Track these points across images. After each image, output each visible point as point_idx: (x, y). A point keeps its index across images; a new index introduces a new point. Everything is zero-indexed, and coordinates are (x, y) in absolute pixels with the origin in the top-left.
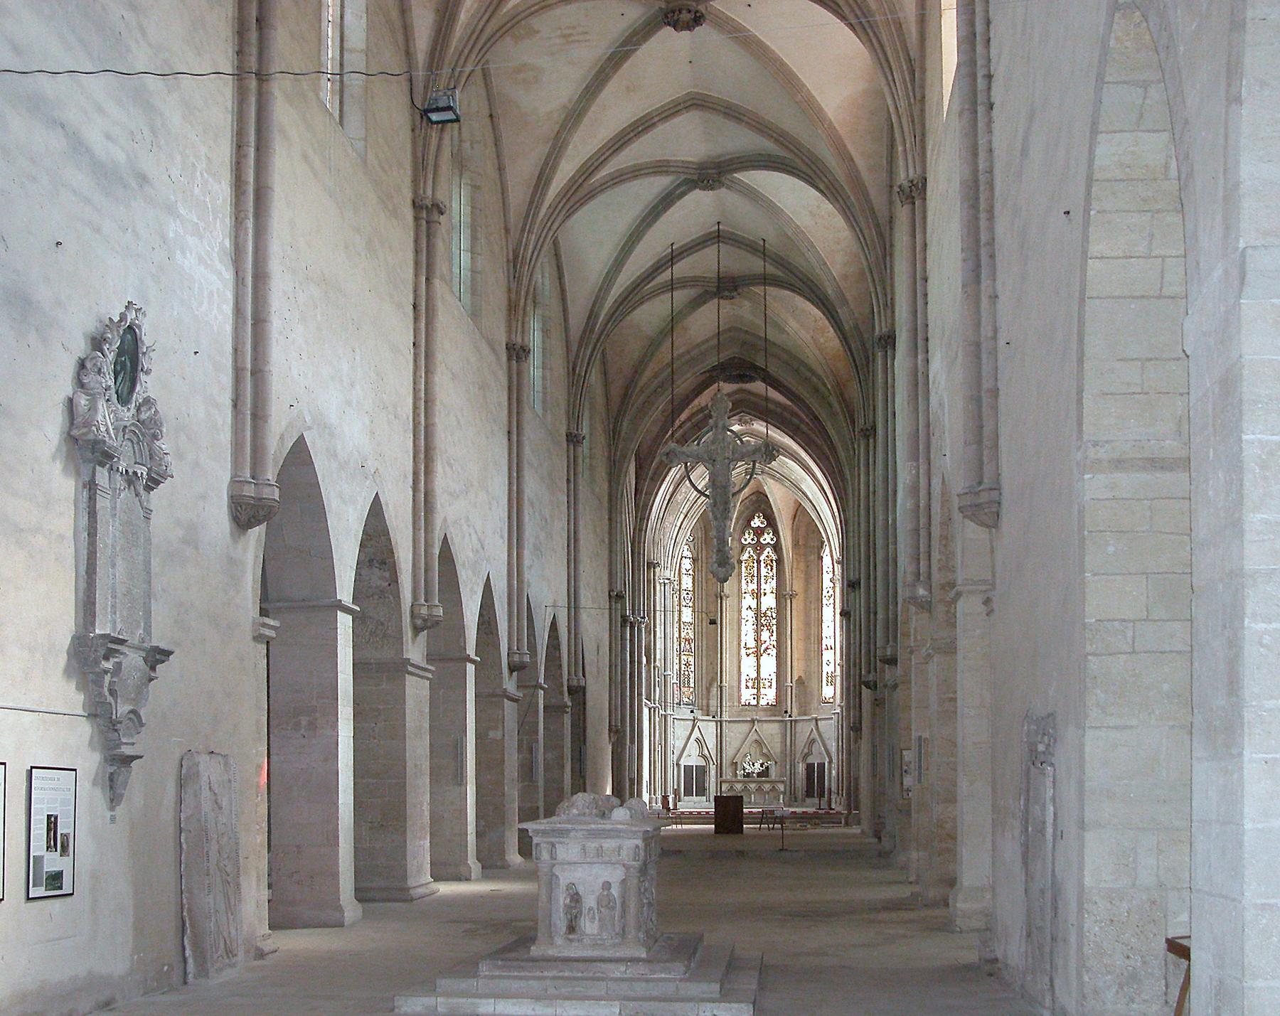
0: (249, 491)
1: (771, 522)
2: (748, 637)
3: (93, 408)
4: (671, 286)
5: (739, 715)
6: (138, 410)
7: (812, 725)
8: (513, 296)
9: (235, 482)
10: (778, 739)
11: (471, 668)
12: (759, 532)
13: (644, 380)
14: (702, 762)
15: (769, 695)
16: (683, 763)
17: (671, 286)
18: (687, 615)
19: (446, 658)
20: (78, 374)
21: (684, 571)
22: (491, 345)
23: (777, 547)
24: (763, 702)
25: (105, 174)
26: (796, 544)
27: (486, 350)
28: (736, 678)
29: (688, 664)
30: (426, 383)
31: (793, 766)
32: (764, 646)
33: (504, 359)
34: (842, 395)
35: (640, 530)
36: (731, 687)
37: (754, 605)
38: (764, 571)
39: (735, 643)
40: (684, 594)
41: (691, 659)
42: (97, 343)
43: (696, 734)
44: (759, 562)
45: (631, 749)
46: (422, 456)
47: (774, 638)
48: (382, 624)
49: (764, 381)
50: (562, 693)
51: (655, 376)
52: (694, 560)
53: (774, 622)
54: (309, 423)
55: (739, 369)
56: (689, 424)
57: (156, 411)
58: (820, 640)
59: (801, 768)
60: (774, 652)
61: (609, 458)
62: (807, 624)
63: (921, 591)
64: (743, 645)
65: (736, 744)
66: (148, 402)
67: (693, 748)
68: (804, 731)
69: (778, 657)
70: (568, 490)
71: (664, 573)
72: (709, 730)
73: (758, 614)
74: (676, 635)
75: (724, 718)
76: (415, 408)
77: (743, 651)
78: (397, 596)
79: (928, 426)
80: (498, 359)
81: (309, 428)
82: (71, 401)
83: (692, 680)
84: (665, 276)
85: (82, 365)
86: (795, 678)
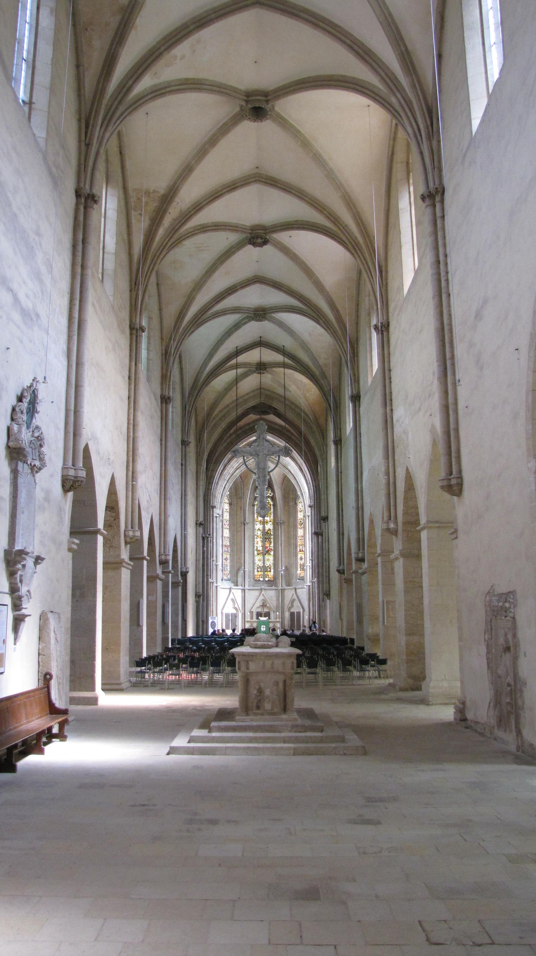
0: (72, 473)
1: (270, 486)
3: (20, 431)
4: (237, 366)
5: (253, 586)
6: (33, 431)
7: (293, 592)
8: (164, 371)
9: (64, 468)
10: (275, 599)
11: (145, 562)
13: (216, 412)
14: (234, 611)
16: (225, 612)
17: (237, 366)
18: (227, 533)
19: (136, 558)
20: (12, 414)
21: (225, 510)
22: (155, 395)
23: (273, 498)
24: (267, 579)
25: (25, 313)
27: (153, 398)
28: (252, 566)
29: (226, 559)
30: (134, 416)
31: (283, 613)
33: (160, 403)
34: (318, 423)
35: (208, 489)
36: (250, 571)
37: (261, 528)
39: (252, 548)
40: (225, 522)
41: (228, 557)
42: (20, 399)
43: (231, 596)
45: (203, 604)
46: (131, 453)
47: (272, 545)
48: (110, 540)
49: (274, 414)
50: (178, 575)
51: (221, 411)
52: (230, 504)
53: (272, 537)
54: (90, 437)
55: (263, 409)
56: (234, 435)
57: (42, 433)
58: (296, 547)
59: (287, 615)
60: (272, 553)
61: (197, 452)
63: (392, 526)
64: (256, 548)
65: (253, 601)
66: (37, 427)
67: (230, 603)
68: (289, 594)
69: (275, 556)
70: (182, 469)
71: (217, 511)
72: (237, 593)
74: (221, 544)
75: (247, 587)
76: (128, 428)
77: (256, 553)
78: (118, 526)
79: (393, 442)
80: (157, 403)
81: (90, 440)
82: (9, 429)
83: (228, 568)
84: (233, 362)
85: (14, 409)
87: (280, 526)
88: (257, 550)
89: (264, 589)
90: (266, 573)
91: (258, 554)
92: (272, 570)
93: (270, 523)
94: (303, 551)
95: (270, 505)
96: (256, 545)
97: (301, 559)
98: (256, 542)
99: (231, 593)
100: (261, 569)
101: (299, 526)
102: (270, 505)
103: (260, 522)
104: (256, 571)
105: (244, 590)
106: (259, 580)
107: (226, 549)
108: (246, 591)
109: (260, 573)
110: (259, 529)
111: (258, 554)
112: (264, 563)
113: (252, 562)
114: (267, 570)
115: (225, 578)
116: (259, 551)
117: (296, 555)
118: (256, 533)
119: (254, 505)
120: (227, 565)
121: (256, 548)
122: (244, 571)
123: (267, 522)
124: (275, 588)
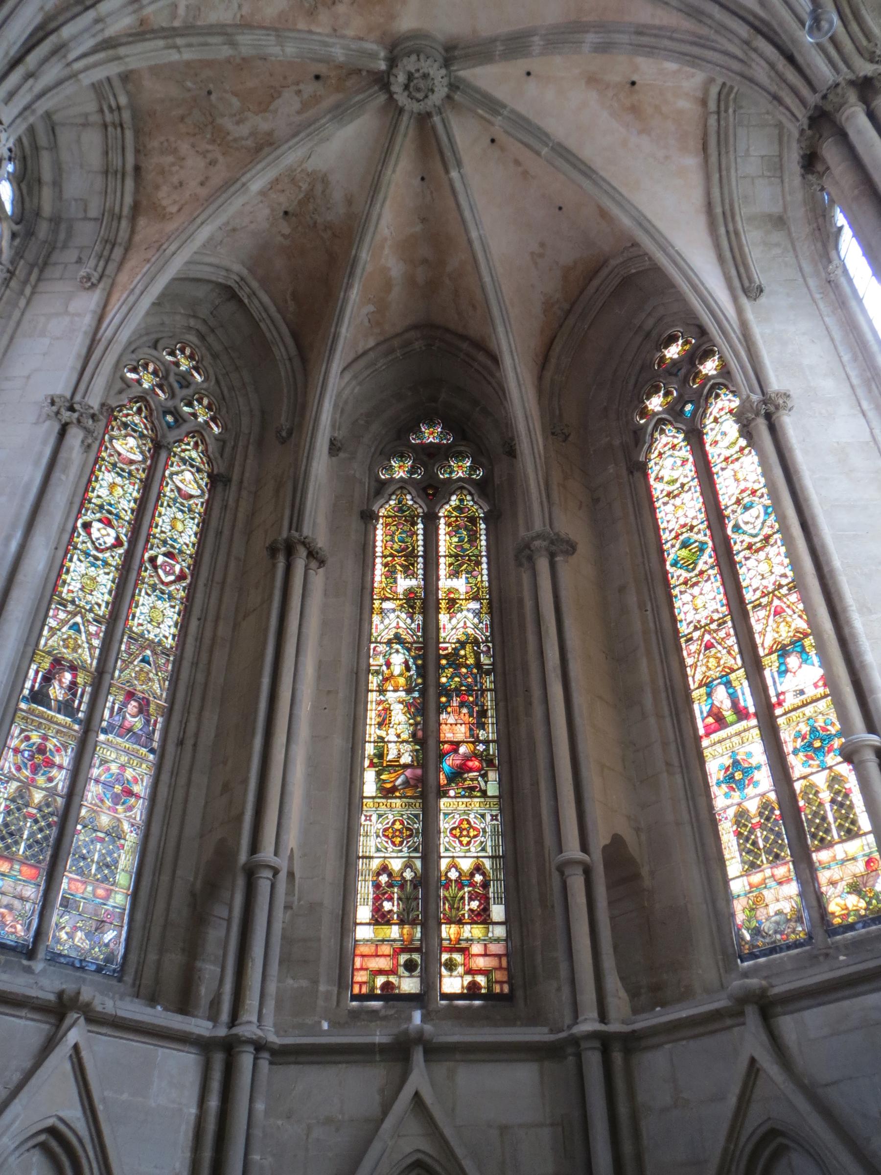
2: (389, 724)
12: (431, 456)
15: (473, 954)
23: (483, 488)
26: (555, 429)
28: (331, 868)
38: (445, 542)
39: (338, 742)
44: (431, 520)
52: (217, 481)
53: (488, 682)
62: (618, 657)
64: (370, 749)
73: (426, 652)
77: (370, 785)
83: (126, 860)
86: (600, 839)
87: (543, 564)
89: (435, 1052)
90: (448, 931)
91: (387, 792)
92: (498, 912)
93: (474, 605)
94: (741, 714)
95: (473, 520)
96: (372, 732)
97: (737, 775)
98: (372, 716)
99: (59, 1062)
100: (406, 899)
101: (677, 575)
102: (473, 520)
103: (410, 598)
104: (364, 913)
105: (221, 1056)
106: (389, 994)
107: (137, 723)
108: (246, 1060)
109: (394, 932)
111: (387, 792)
112: (428, 851)
113: (333, 837)
114: (455, 903)
115: (69, 935)
116: (395, 766)
117: (692, 759)
118: (377, 662)
119: (369, 517)
120: (115, 834)
121: (370, 749)
122: (251, 874)
123: (452, 603)
124: (538, 1034)
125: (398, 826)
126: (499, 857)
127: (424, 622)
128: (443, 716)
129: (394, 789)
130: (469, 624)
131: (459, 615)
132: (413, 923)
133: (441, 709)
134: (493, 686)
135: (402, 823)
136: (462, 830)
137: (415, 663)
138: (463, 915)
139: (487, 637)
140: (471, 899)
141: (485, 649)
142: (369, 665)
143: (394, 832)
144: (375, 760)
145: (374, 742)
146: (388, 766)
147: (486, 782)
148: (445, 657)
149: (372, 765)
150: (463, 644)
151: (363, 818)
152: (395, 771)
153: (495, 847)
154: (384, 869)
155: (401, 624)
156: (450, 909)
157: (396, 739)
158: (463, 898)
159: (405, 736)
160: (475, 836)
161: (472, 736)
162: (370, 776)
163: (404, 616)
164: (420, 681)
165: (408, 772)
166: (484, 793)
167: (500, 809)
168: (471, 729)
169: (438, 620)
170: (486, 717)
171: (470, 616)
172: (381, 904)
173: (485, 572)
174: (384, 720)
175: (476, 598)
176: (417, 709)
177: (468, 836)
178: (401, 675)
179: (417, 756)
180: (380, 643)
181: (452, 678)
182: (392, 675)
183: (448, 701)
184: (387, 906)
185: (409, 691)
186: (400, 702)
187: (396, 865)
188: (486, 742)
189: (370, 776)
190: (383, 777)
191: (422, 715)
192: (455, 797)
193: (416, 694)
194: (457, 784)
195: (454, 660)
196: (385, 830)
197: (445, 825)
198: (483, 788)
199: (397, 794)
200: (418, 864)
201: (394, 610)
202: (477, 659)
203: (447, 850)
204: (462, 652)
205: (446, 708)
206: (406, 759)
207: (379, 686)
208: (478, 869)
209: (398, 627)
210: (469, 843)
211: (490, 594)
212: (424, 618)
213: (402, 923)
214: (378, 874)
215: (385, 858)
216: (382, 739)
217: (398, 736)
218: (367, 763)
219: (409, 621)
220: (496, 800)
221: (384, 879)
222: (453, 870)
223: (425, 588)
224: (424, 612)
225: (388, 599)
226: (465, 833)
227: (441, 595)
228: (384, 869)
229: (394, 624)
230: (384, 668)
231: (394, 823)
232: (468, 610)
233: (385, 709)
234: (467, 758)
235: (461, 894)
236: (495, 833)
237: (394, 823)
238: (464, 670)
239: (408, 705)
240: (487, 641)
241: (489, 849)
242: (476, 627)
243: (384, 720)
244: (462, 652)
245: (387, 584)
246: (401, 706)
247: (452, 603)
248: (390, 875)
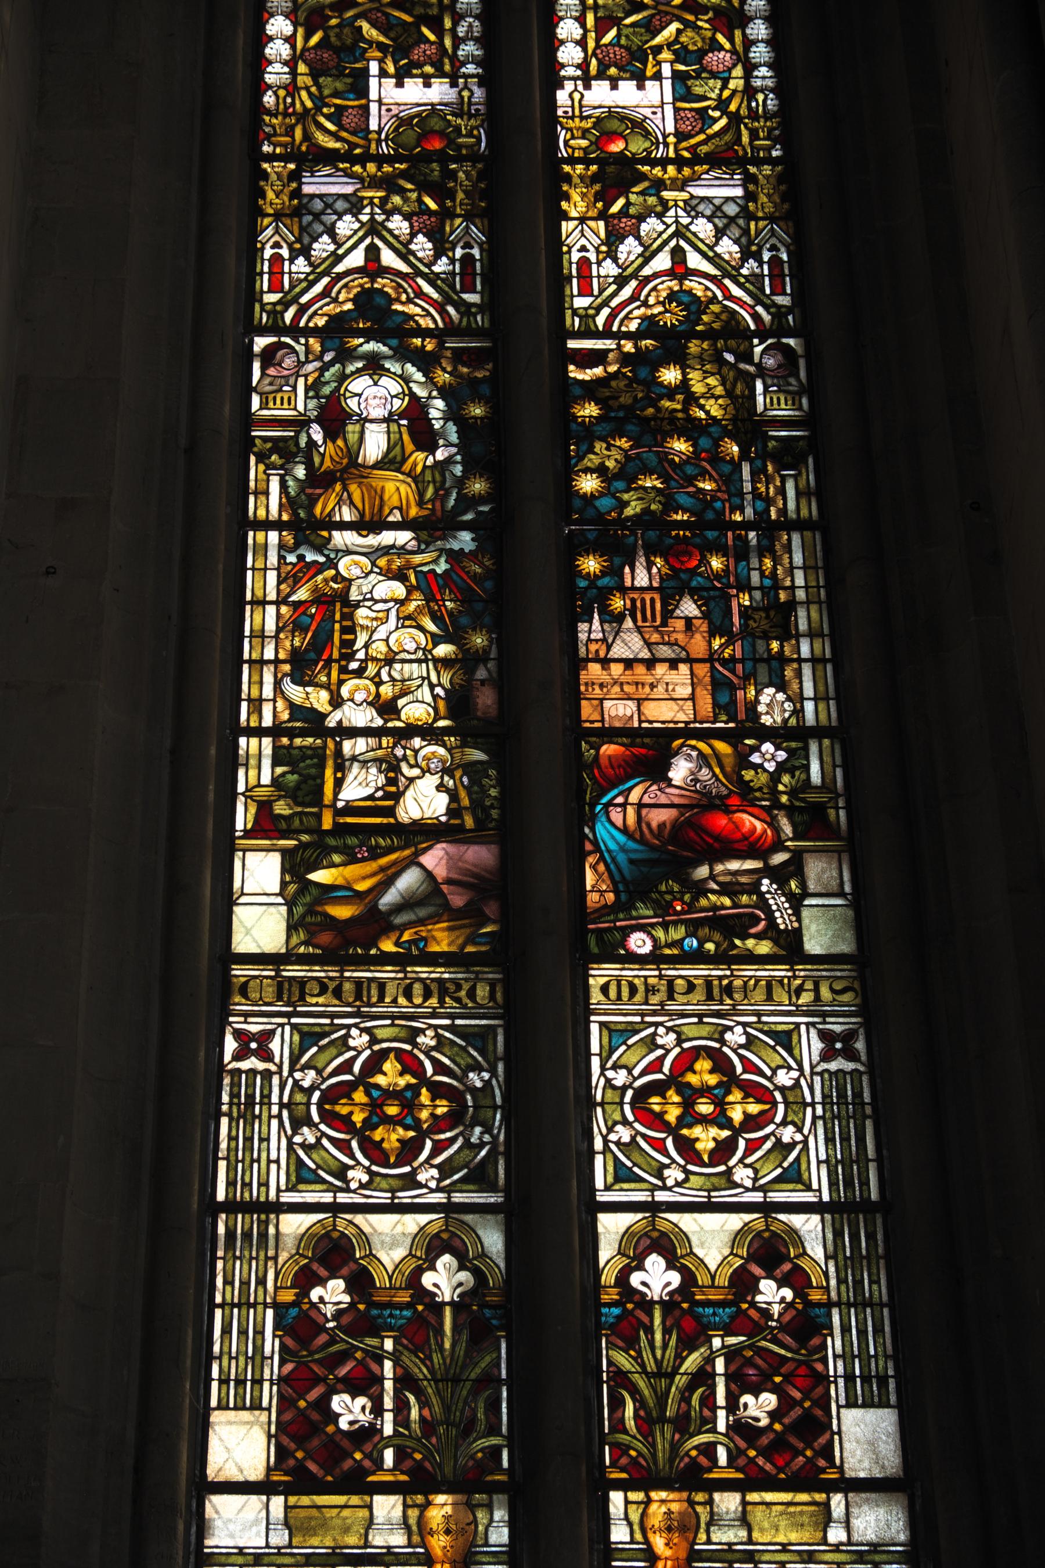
32: (628, 813)
64: (259, 767)
73: (508, 352)
88: (308, 830)
92: (865, 1436)
103: (420, 155)
104: (238, 1444)
110: (374, 314)
111: (334, 938)
112: (537, 1171)
118: (282, 400)
123: (615, 176)
125: (390, 1075)
126: (865, 1206)
127: (491, 249)
128: (591, 630)
129: (375, 922)
130: (694, 260)
131: (651, 226)
132: (471, 1485)
133: (585, 600)
134: (811, 510)
135: (409, 1064)
136: (690, 1096)
137: (452, 415)
138: (709, 1450)
139: (779, 314)
140: (741, 1383)
141: (770, 362)
142: (248, 420)
143: (375, 1107)
144: (281, 808)
145: (275, 731)
146: (339, 830)
147: (796, 903)
148: (591, 390)
149: (267, 826)
150: (670, 344)
151: (230, 1045)
152: (375, 854)
153: (845, 1168)
154: (332, 1253)
155: (388, 258)
156: (647, 1423)
157: (379, 722)
158: (704, 1377)
159: (415, 710)
160: (751, 1122)
161: (724, 707)
162: (260, 871)
163: (398, 225)
164: (478, 486)
165: (435, 858)
166: (790, 947)
167: (864, 1010)
168: (718, 684)
169: (556, 245)
170: (787, 632)
171: (703, 228)
172: (323, 1404)
173: (760, 53)
174: (320, 643)
175: (723, 159)
176: (466, 598)
177: (720, 1119)
178: (391, 461)
179: (476, 790)
180: (294, 331)
181: (626, 475)
182: (352, 468)
183: (614, 571)
184: (349, 1410)
185: (430, 528)
186: (390, 574)
187: (390, 1238)
188: (793, 736)
189: (260, 871)
190: (321, 876)
191: (498, 629)
192: (655, 958)
193: (465, 540)
194: (663, 909)
195: (637, 410)
196: (331, 1096)
197: (613, 1072)
198: (783, 920)
199: (388, 946)
200: (493, 1240)
201: (355, 205)
202: (741, 401)
203: (622, 1176)
204: (670, 375)
205: (603, 596)
206: (425, 800)
207: (289, 502)
208: (769, 1251)
209: (373, 267)
210: (723, 1151)
211: (784, 140)
212: (490, 233)
213: (417, 1485)
214: (306, 1280)
215: (335, 1208)
216: (311, 721)
217: (388, 708)
218: (243, 818)
219: (422, 246)
220: (843, 971)
221: (333, 1293)
222: (655, 1262)
223: (494, 115)
224: (493, 207)
225: (330, 157)
226: (705, 1108)
227: (569, 142)
228: (332, 1253)
229: (357, 259)
230: (317, 433)
231: (374, 1065)
232: (692, 207)
233: (321, 599)
234: (702, 803)
235: (692, 1361)
236: (840, 1105)
237: (374, 1065)
238: (681, 446)
239: (428, 586)
240: (779, 329)
241: (819, 1177)
242: (728, 271)
243: (320, 643)
244: (670, 375)
245: (320, 102)
246: (399, 590)
247: (615, 176)
248: (360, 1283)
